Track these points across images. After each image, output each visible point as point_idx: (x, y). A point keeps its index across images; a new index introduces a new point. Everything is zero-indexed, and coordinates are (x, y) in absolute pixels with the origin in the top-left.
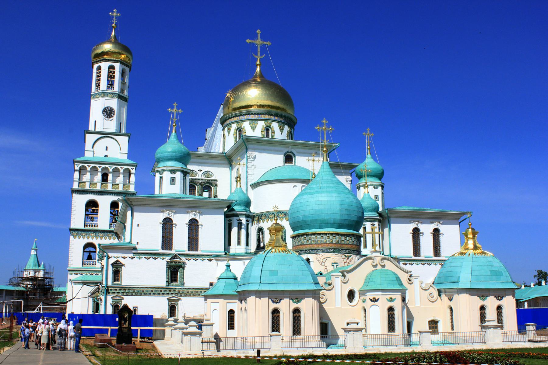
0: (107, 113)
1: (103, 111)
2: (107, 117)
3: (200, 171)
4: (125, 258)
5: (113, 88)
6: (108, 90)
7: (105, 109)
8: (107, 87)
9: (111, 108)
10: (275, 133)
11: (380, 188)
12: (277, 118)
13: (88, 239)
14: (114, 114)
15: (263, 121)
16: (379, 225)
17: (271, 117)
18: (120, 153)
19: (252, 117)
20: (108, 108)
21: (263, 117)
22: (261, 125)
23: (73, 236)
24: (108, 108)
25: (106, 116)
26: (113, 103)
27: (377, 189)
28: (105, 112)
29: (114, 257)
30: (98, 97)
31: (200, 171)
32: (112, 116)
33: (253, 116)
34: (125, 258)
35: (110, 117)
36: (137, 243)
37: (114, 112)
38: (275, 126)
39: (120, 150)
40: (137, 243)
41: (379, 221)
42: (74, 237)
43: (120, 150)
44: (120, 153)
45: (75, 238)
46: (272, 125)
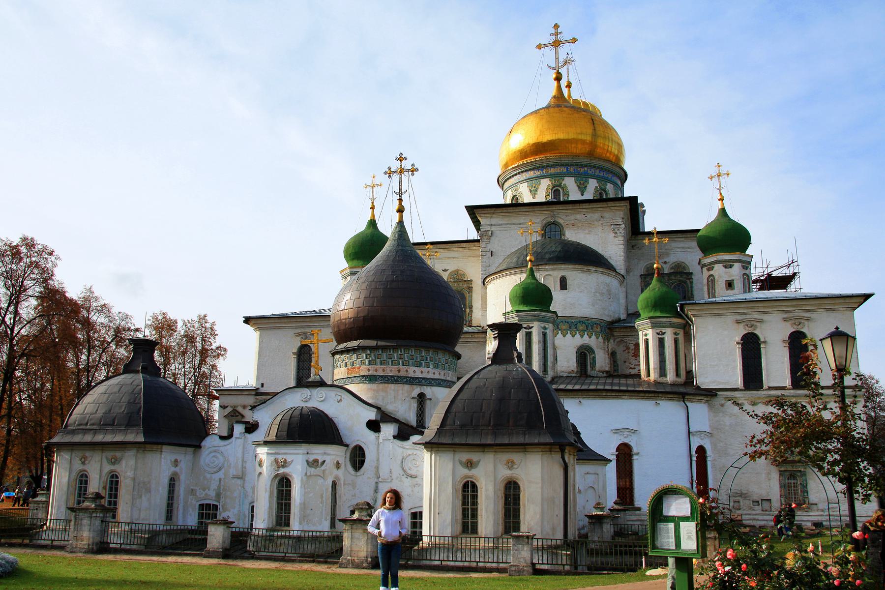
3: (445, 270)
4: (244, 407)
10: (570, 194)
11: (737, 266)
12: (572, 170)
15: (549, 179)
16: (675, 334)
17: (562, 169)
19: (531, 174)
21: (547, 171)
22: (545, 183)
27: (731, 268)
29: (231, 407)
31: (445, 270)
33: (532, 172)
34: (244, 407)
36: (262, 385)
38: (570, 183)
40: (262, 385)
41: (671, 325)
46: (563, 183)
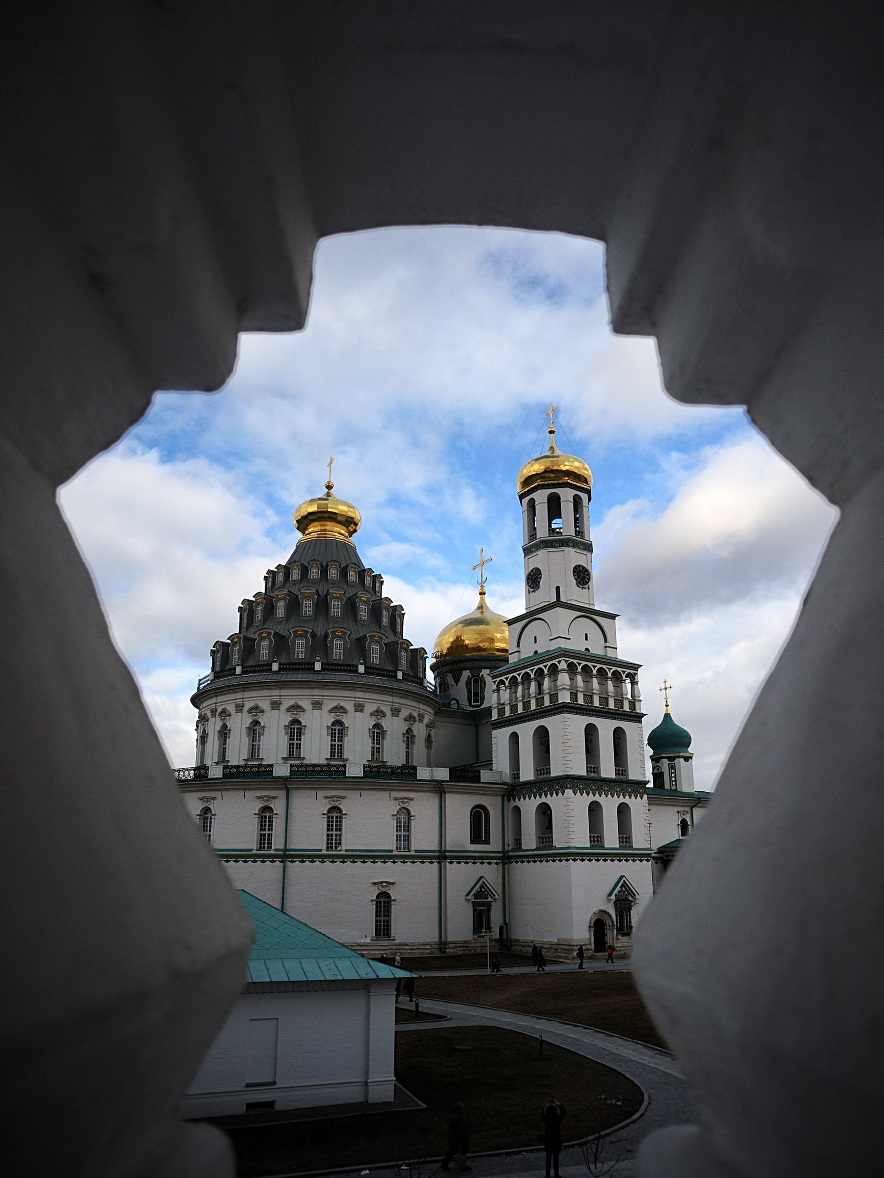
1: (574, 571)
2: (580, 583)
7: (575, 568)
9: (583, 567)
14: (589, 579)
20: (580, 569)
24: (579, 566)
30: (559, 547)
32: (587, 583)
35: (584, 584)
39: (606, 641)
42: (573, 792)
43: (606, 641)
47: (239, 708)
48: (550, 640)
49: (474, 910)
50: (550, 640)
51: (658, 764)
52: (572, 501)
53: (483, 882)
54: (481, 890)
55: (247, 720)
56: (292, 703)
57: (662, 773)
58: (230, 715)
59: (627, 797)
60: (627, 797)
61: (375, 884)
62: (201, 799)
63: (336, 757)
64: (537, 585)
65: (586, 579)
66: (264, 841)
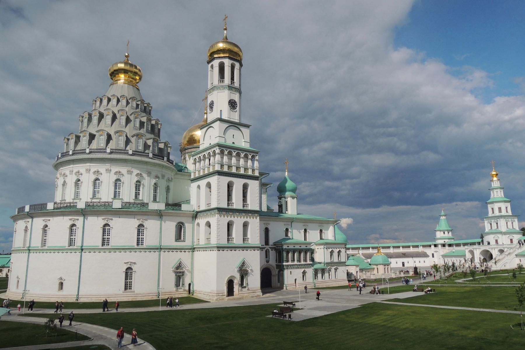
0: (232, 105)
1: (229, 102)
2: (232, 108)
5: (224, 81)
6: (220, 83)
7: (230, 101)
8: (219, 81)
9: (234, 101)
13: (231, 217)
14: (237, 107)
18: (244, 142)
20: (232, 101)
23: (219, 215)
24: (232, 100)
25: (231, 107)
26: (236, 97)
28: (230, 104)
35: (234, 109)
37: (237, 104)
42: (220, 215)
44: (244, 142)
45: (221, 217)
47: (71, 172)
48: (215, 138)
49: (176, 275)
50: (215, 138)
51: (280, 200)
52: (230, 66)
53: (181, 261)
54: (180, 265)
55: (75, 178)
56: (96, 169)
57: (282, 205)
58: (67, 176)
59: (248, 218)
60: (248, 218)
61: (125, 263)
62: (70, 220)
63: (117, 198)
64: (212, 109)
65: (235, 107)
66: (71, 242)
